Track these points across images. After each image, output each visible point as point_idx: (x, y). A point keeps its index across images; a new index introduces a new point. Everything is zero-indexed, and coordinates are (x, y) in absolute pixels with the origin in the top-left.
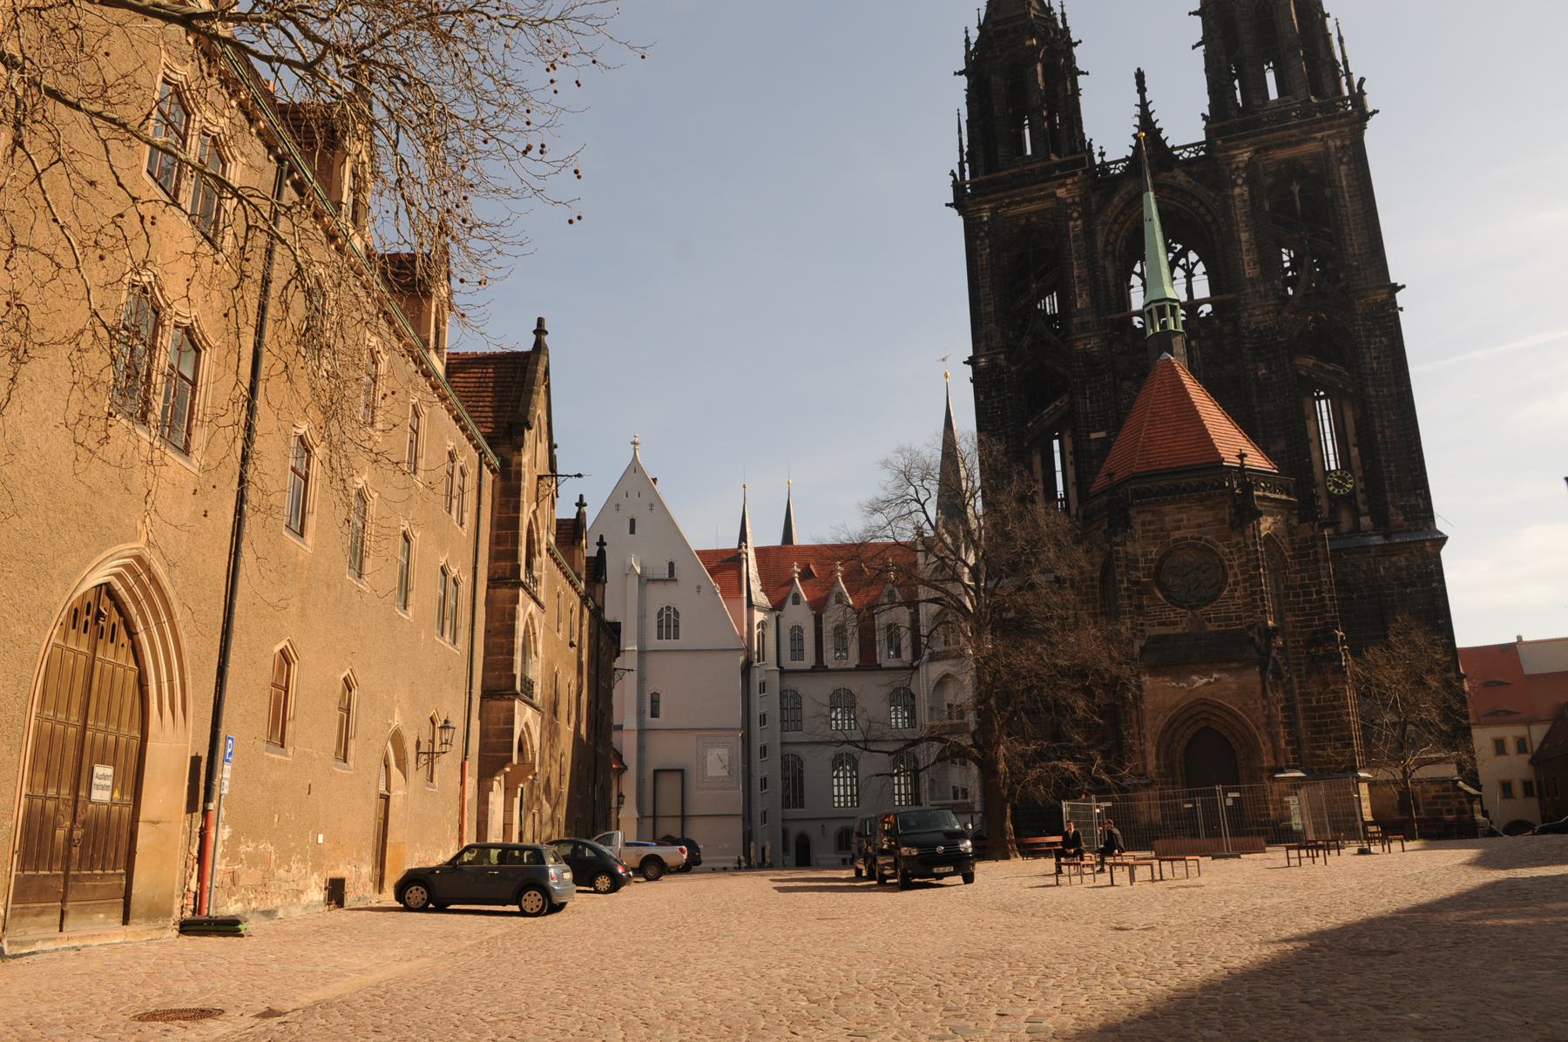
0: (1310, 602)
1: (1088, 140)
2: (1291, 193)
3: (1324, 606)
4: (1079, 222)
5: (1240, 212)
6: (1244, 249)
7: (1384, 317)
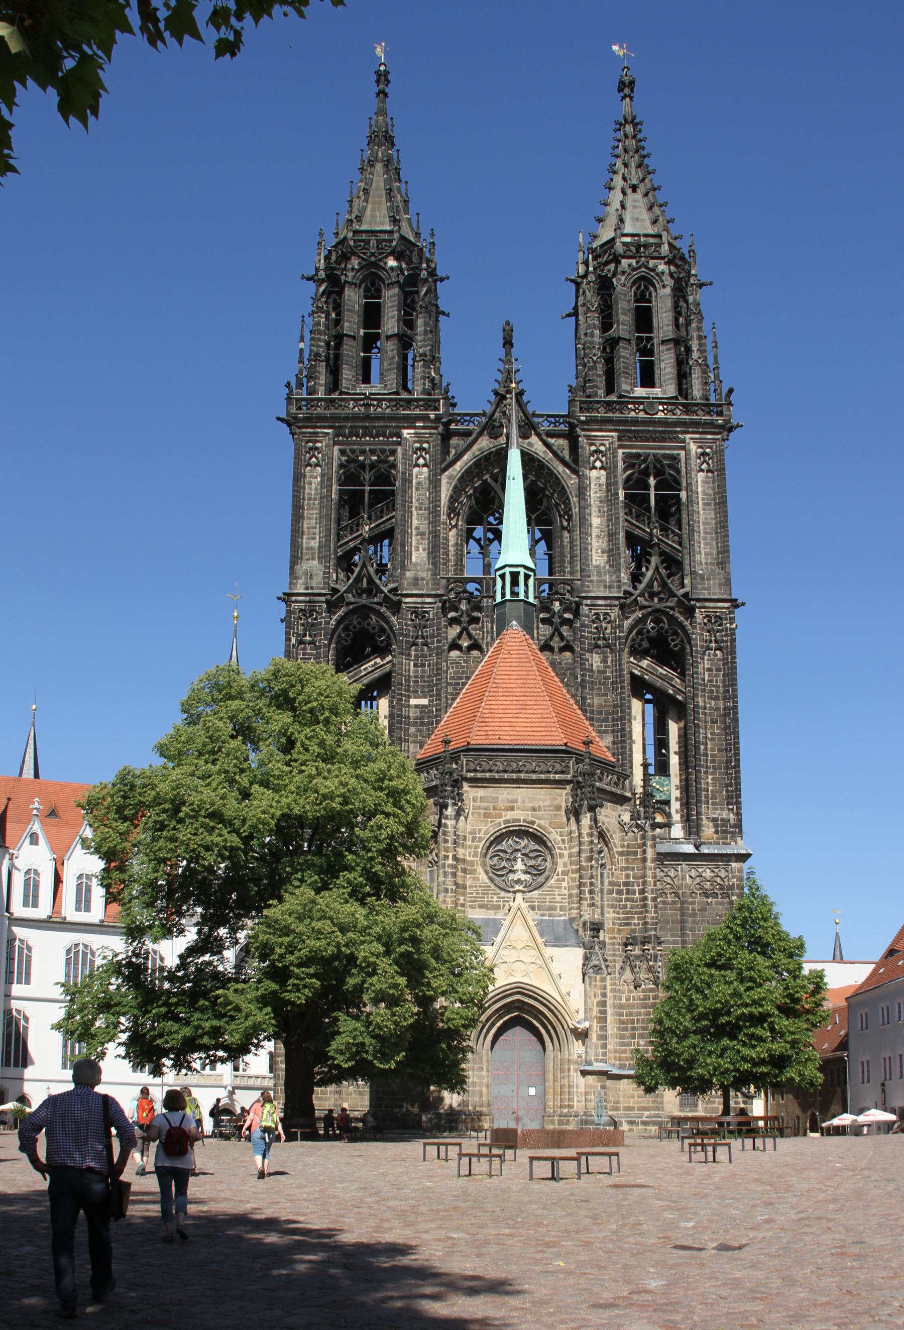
0: (632, 900)
1: (444, 384)
2: (647, 487)
3: (645, 906)
4: (425, 469)
5: (595, 495)
6: (594, 535)
7: (722, 631)
